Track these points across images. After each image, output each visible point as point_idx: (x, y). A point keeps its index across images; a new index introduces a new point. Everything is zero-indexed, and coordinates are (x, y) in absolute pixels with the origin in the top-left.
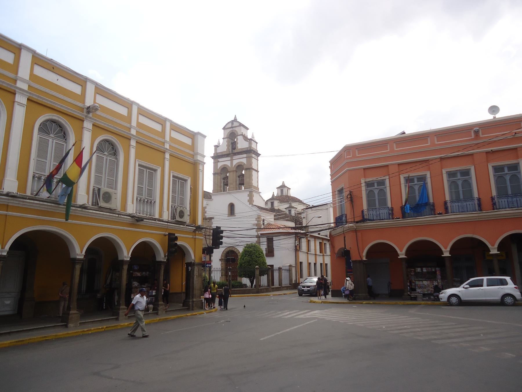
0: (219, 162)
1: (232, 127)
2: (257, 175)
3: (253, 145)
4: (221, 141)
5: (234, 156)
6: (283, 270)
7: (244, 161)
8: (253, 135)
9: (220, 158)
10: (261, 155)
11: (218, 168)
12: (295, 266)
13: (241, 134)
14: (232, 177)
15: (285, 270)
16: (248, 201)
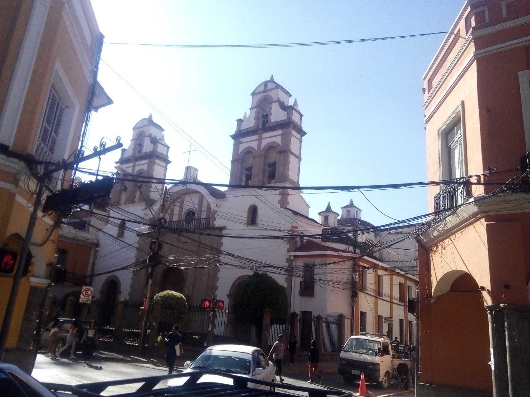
0: (241, 142)
1: (265, 91)
2: (298, 164)
3: (295, 118)
4: (248, 112)
5: (264, 133)
6: (324, 322)
7: (278, 140)
8: (296, 101)
9: (242, 137)
10: (307, 134)
11: (240, 152)
12: (351, 318)
13: (278, 100)
14: (258, 166)
15: (330, 322)
16: (279, 202)
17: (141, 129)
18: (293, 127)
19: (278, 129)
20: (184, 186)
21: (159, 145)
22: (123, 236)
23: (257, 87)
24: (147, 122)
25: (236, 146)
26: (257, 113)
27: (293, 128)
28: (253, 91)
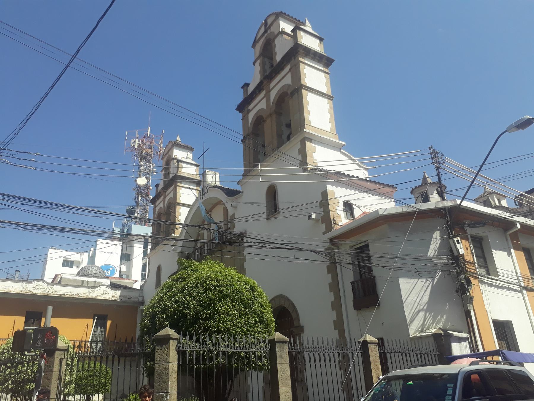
0: (249, 111)
1: (266, 31)
7: (288, 80)
9: (249, 104)
17: (168, 154)
18: (303, 52)
19: (285, 65)
20: (203, 199)
21: (184, 165)
22: (160, 285)
23: (257, 34)
24: (171, 145)
25: (245, 119)
26: (263, 65)
27: (303, 53)
28: (254, 39)
